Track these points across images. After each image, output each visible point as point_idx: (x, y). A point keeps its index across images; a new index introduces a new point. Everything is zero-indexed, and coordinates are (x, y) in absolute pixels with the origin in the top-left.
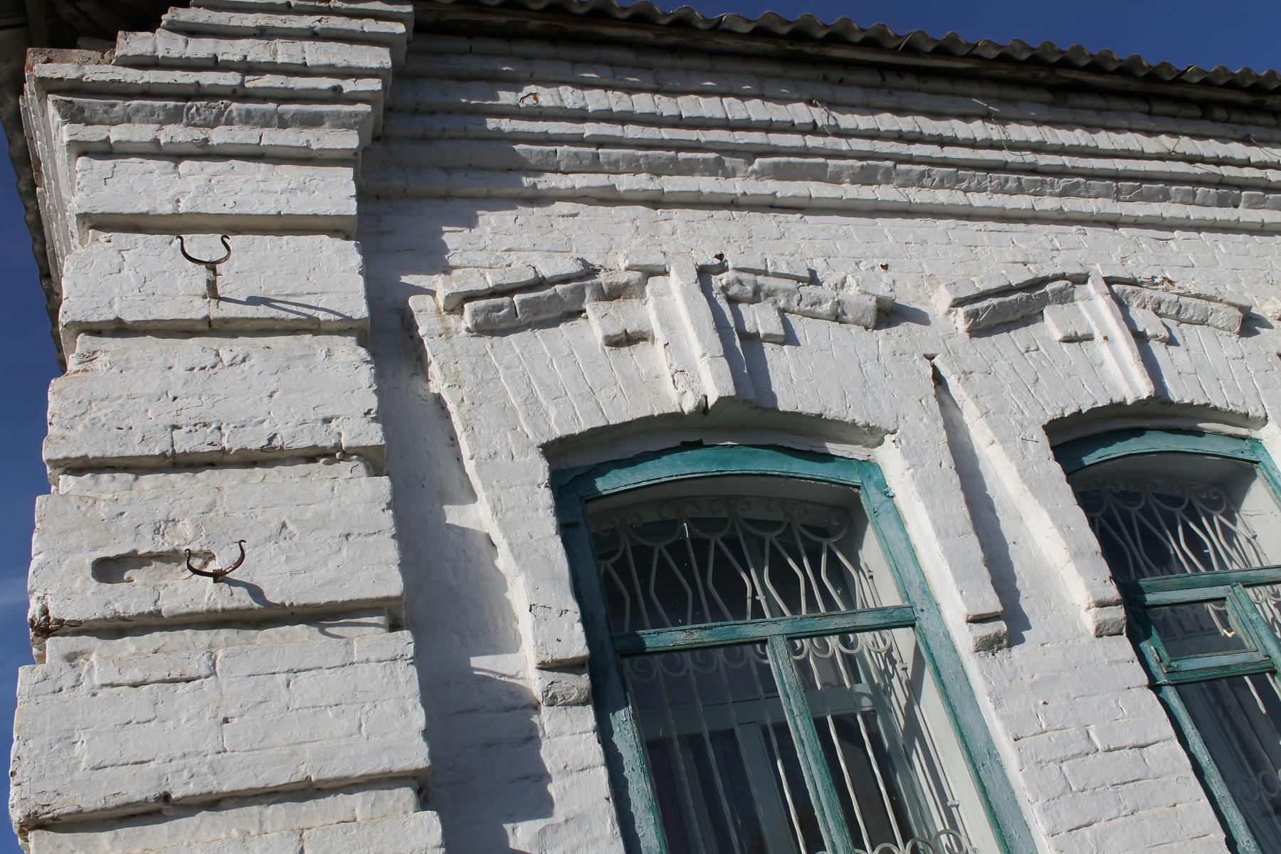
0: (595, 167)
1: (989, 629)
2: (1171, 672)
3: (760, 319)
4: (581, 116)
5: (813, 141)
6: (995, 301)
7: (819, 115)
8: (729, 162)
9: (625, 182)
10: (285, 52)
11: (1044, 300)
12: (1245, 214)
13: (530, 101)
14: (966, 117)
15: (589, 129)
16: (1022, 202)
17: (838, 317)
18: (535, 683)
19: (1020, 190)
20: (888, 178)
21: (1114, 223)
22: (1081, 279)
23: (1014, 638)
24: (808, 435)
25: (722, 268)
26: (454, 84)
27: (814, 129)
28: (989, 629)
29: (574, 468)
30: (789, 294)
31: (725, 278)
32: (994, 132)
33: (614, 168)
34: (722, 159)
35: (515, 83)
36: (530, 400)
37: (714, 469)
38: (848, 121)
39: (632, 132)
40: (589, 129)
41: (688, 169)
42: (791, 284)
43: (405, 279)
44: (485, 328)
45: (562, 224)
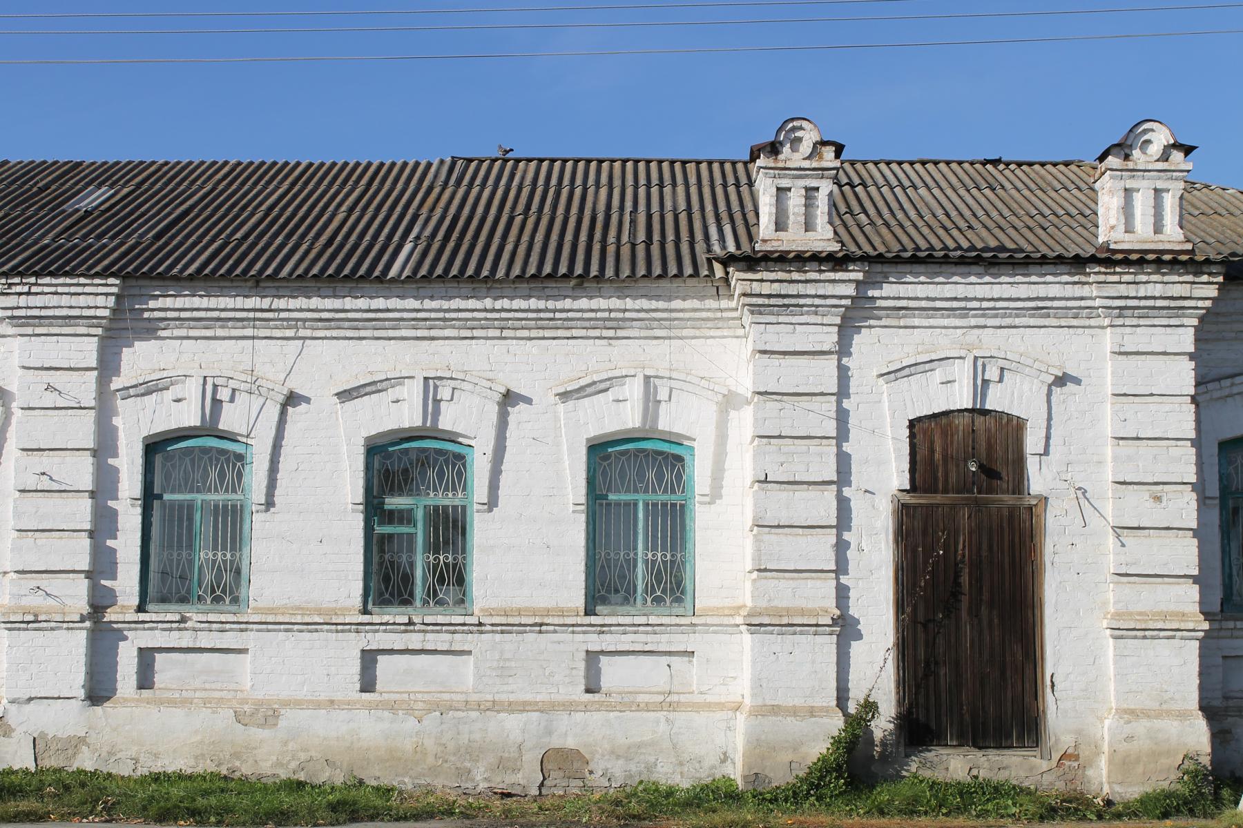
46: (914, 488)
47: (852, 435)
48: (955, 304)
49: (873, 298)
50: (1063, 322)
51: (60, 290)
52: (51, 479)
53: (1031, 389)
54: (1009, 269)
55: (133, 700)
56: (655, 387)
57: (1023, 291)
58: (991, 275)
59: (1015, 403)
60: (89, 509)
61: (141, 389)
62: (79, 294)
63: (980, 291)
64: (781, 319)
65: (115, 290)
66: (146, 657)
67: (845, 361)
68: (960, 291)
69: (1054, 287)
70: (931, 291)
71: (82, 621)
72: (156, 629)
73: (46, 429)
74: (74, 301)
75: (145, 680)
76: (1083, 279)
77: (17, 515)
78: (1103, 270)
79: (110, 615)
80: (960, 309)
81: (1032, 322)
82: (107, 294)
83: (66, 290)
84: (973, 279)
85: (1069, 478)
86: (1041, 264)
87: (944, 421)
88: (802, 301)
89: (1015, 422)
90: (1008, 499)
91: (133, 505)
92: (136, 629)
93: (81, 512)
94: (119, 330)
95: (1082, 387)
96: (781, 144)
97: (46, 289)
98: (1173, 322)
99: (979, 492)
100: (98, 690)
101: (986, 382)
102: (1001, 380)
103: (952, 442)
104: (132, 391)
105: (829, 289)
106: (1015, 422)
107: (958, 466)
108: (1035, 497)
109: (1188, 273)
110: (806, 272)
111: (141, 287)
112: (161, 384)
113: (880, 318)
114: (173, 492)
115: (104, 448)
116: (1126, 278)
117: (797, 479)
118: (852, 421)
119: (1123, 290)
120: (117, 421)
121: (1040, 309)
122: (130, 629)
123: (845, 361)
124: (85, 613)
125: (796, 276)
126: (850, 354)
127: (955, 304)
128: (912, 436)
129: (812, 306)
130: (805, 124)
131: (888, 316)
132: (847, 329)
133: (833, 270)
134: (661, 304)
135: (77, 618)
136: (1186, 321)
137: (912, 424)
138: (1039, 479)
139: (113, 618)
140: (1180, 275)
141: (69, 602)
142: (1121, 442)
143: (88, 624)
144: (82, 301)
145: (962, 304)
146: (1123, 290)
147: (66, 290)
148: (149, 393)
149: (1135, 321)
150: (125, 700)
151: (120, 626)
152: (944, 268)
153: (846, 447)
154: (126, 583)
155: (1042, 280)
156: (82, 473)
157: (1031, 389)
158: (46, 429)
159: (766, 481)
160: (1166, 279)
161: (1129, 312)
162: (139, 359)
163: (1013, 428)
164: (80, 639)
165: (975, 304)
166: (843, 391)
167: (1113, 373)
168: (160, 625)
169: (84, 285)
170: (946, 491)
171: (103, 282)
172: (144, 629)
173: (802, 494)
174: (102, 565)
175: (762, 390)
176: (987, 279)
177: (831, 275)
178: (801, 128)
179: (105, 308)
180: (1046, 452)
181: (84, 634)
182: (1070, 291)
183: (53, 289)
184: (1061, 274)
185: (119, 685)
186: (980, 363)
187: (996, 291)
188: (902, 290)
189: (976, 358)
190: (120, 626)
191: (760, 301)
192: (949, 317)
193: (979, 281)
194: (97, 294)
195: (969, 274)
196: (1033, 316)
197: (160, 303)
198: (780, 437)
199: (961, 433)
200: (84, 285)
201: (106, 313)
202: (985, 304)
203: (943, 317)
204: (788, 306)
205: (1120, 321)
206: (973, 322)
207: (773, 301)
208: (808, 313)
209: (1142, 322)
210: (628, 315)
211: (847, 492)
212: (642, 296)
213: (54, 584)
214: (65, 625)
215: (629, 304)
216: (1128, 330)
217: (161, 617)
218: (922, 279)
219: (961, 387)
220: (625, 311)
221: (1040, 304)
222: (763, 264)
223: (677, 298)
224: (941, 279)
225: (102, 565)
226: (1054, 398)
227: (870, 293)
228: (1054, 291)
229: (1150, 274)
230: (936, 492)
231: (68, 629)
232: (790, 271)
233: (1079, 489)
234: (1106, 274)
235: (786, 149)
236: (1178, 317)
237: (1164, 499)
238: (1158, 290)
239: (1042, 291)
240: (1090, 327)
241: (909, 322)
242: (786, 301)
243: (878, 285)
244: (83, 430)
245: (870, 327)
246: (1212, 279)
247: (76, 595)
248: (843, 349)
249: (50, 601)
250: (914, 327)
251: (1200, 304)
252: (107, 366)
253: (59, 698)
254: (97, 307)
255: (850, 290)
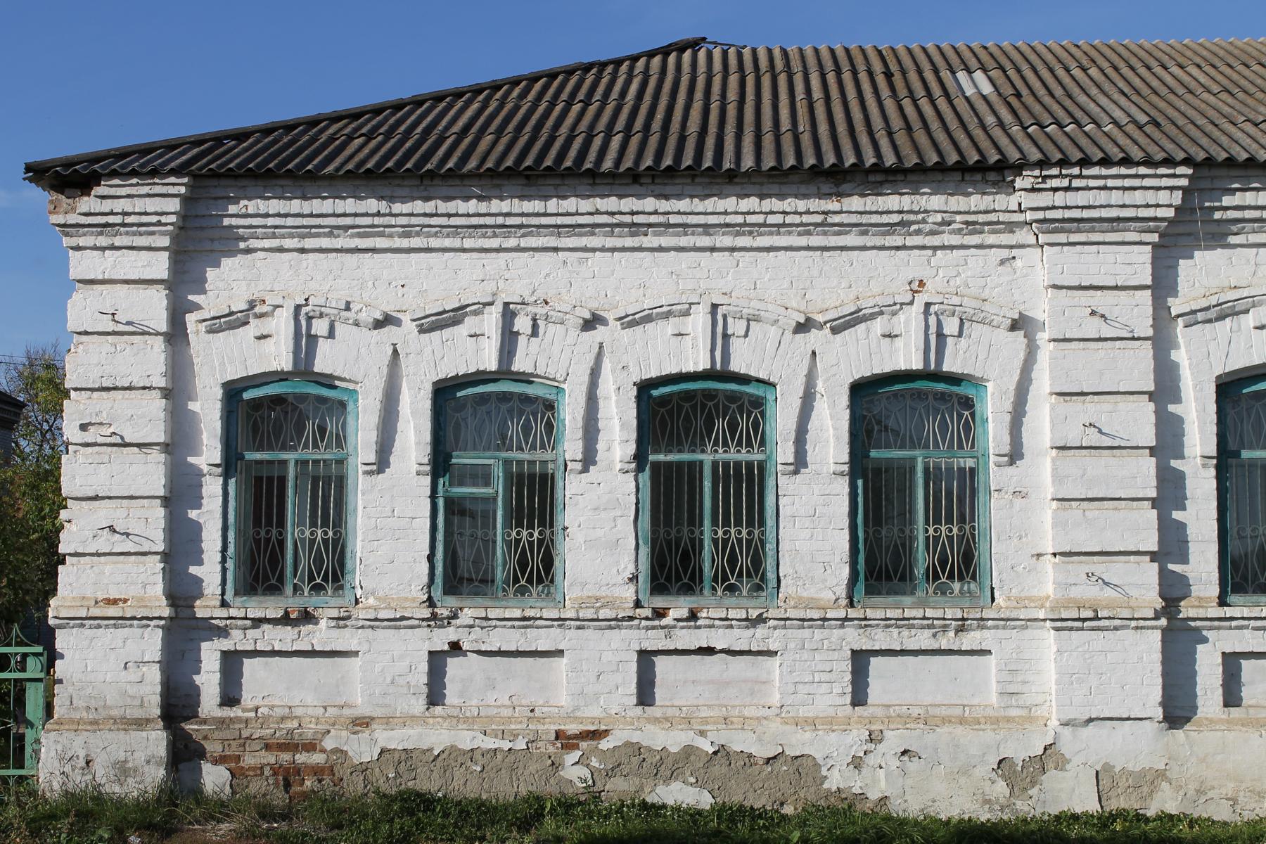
0: (274, 236)
1: (369, 468)
2: (447, 491)
3: (320, 327)
4: (267, 215)
5: (377, 221)
6: (434, 318)
7: (383, 206)
8: (336, 232)
9: (288, 243)
10: (139, 205)
11: (466, 314)
12: (650, 241)
13: (244, 210)
14: (467, 198)
15: (270, 222)
16: (494, 243)
17: (357, 324)
18: (205, 469)
19: (495, 236)
20: (418, 234)
21: (556, 249)
22: (491, 304)
23: (380, 470)
24: (327, 381)
25: (307, 305)
26: (212, 202)
27: (378, 214)
28: (369, 468)
29: (232, 392)
30: (335, 315)
31: (308, 309)
32: (483, 207)
33: (283, 237)
34: (332, 231)
35: (236, 201)
36: (222, 364)
37: (290, 391)
38: (397, 208)
39: (290, 221)
40: (270, 222)
41: (317, 235)
42: (336, 312)
43: (190, 297)
44: (211, 331)
45: (259, 264)
51: (1110, 183)
52: (1100, 431)
55: (1221, 721)
60: (1153, 471)
61: (1212, 314)
62: (1135, 189)
65: (1184, 182)
66: (1232, 663)
71: (1156, 618)
72: (1247, 627)
73: (1092, 368)
74: (1128, 198)
75: (1232, 697)
77: (1057, 478)
79: (1187, 610)
82: (1172, 188)
83: (1118, 183)
91: (1204, 466)
92: (1219, 628)
93: (1142, 475)
94: (1178, 237)
97: (1092, 183)
100: (1177, 712)
104: (1200, 316)
111: (1213, 178)
112: (1240, 306)
114: (1251, 448)
115: (1165, 389)
120: (1174, 355)
122: (1211, 628)
124: (1159, 607)
135: (1151, 615)
139: (1192, 613)
141: (1134, 592)
143: (1163, 622)
144: (1139, 197)
147: (1118, 183)
148: (1221, 318)
150: (1211, 721)
151: (1198, 623)
154: (1203, 566)
156: (1140, 424)
158: (1092, 368)
162: (1202, 273)
164: (1154, 639)
168: (1252, 623)
169: (1144, 176)
171: (1171, 171)
172: (1230, 628)
174: (1172, 543)
179: (1170, 206)
181: (1158, 635)
183: (1100, 183)
185: (1200, 702)
190: (1198, 623)
194: (1159, 188)
197: (1237, 199)
200: (1144, 176)
201: (1170, 213)
213: (1114, 570)
214: (1133, 624)
217: (1246, 612)
225: (1172, 543)
231: (1137, 628)
244: (1137, 368)
247: (1142, 584)
249: (1109, 593)
252: (1162, 285)
253: (1128, 719)
254: (1158, 206)
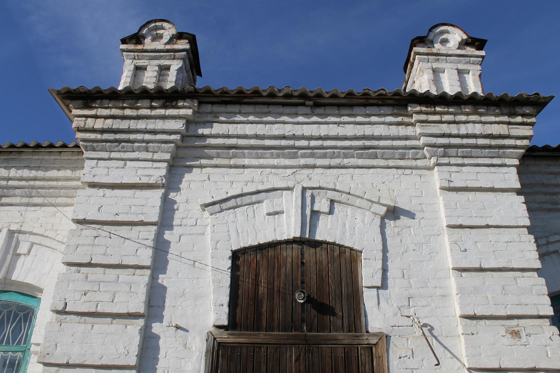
46: (233, 324)
47: (171, 266)
48: (284, 143)
49: (204, 137)
50: (391, 163)
53: (363, 221)
54: (335, 111)
56: (18, 242)
57: (349, 130)
58: (318, 115)
59: (348, 234)
63: (308, 130)
64: (113, 155)
67: (172, 195)
68: (288, 130)
69: (379, 126)
70: (260, 129)
76: (406, 120)
78: (424, 109)
80: (287, 148)
81: (361, 162)
84: (301, 119)
85: (412, 313)
86: (365, 105)
87: (271, 253)
88: (132, 137)
89: (348, 254)
90: (343, 337)
95: (416, 221)
96: (144, 37)
98: (496, 161)
99: (310, 330)
101: (315, 214)
102: (331, 212)
103: (279, 276)
105: (159, 125)
106: (348, 254)
107: (285, 300)
108: (375, 335)
109: (502, 114)
110: (138, 108)
113: (211, 158)
116: (446, 118)
117: (100, 309)
118: (173, 250)
119: (445, 128)
121: (368, 149)
123: (172, 195)
125: (128, 112)
126: (178, 190)
127: (284, 143)
128: (235, 268)
129: (143, 141)
130: (165, 25)
131: (218, 156)
132: (177, 168)
133: (165, 107)
134: (40, 174)
136: (508, 161)
137: (236, 255)
138: (378, 316)
140: (496, 115)
142: (464, 274)
145: (291, 143)
146: (445, 128)
149: (460, 161)
152: (272, 108)
153: (162, 279)
155: (367, 120)
157: (363, 221)
159: (63, 312)
160: (484, 119)
161: (452, 151)
163: (345, 260)
165: (304, 143)
166: (165, 220)
167: (445, 205)
170: (270, 328)
173: (102, 326)
175: (81, 217)
176: (315, 119)
177: (162, 112)
178: (162, 28)
180: (384, 286)
182: (394, 131)
184: (385, 115)
186: (308, 193)
187: (324, 130)
188: (232, 129)
189: (304, 189)
191: (93, 136)
192: (278, 156)
193: (306, 120)
195: (297, 115)
196: (360, 157)
198: (90, 265)
199: (289, 266)
202: (313, 143)
203: (272, 156)
204: (119, 141)
205: (445, 160)
206: (302, 161)
207: (106, 136)
208: (139, 149)
209: (466, 161)
210: (11, 183)
211: (156, 328)
212: (25, 167)
215: (13, 173)
216: (454, 169)
218: (251, 118)
219: (289, 217)
220: (8, 179)
221: (368, 143)
222: (98, 101)
223: (53, 168)
224: (270, 119)
226: (388, 231)
227: (200, 131)
228: (379, 130)
229: (468, 114)
230: (259, 329)
232: (123, 108)
233: (425, 325)
234: (427, 113)
235: (148, 40)
236: (499, 157)
237: (523, 334)
238: (478, 129)
239: (368, 130)
240: (417, 168)
241: (240, 161)
242: (118, 136)
243: (210, 124)
245: (202, 167)
246: (525, 120)
248: (171, 183)
250: (244, 167)
251: (519, 143)
255: (179, 125)
